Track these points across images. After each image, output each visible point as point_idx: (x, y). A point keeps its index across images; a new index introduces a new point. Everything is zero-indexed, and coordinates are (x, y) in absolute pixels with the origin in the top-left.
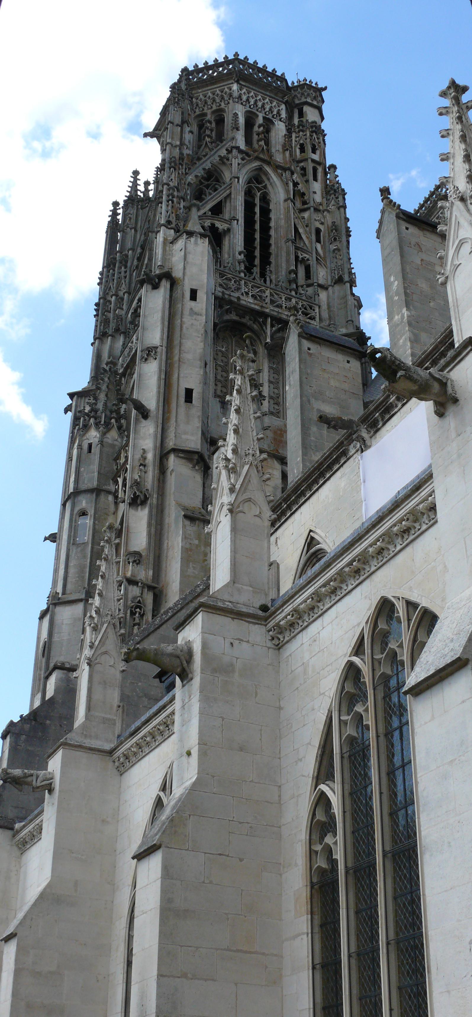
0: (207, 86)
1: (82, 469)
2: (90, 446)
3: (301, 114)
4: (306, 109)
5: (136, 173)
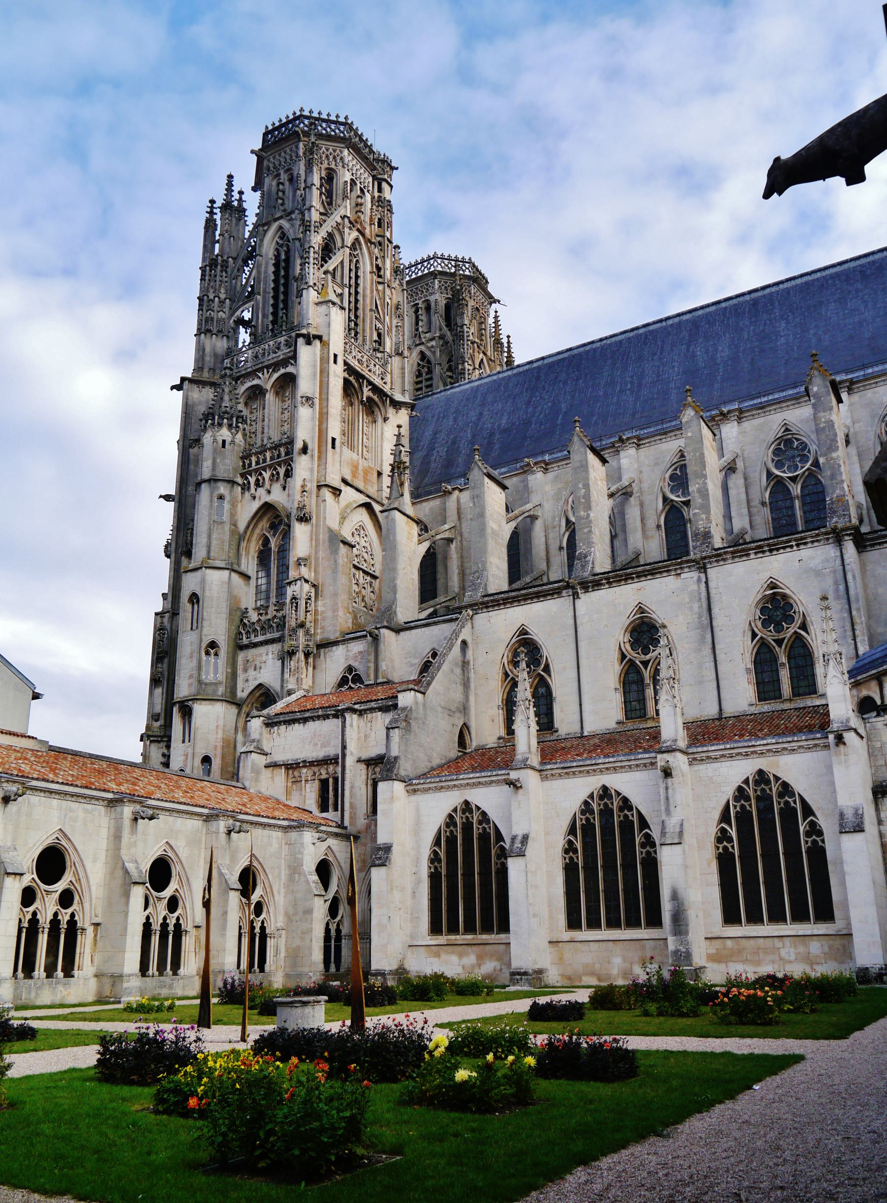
0: (322, 139)
2: (224, 442)
3: (380, 190)
4: (384, 185)
5: (230, 177)
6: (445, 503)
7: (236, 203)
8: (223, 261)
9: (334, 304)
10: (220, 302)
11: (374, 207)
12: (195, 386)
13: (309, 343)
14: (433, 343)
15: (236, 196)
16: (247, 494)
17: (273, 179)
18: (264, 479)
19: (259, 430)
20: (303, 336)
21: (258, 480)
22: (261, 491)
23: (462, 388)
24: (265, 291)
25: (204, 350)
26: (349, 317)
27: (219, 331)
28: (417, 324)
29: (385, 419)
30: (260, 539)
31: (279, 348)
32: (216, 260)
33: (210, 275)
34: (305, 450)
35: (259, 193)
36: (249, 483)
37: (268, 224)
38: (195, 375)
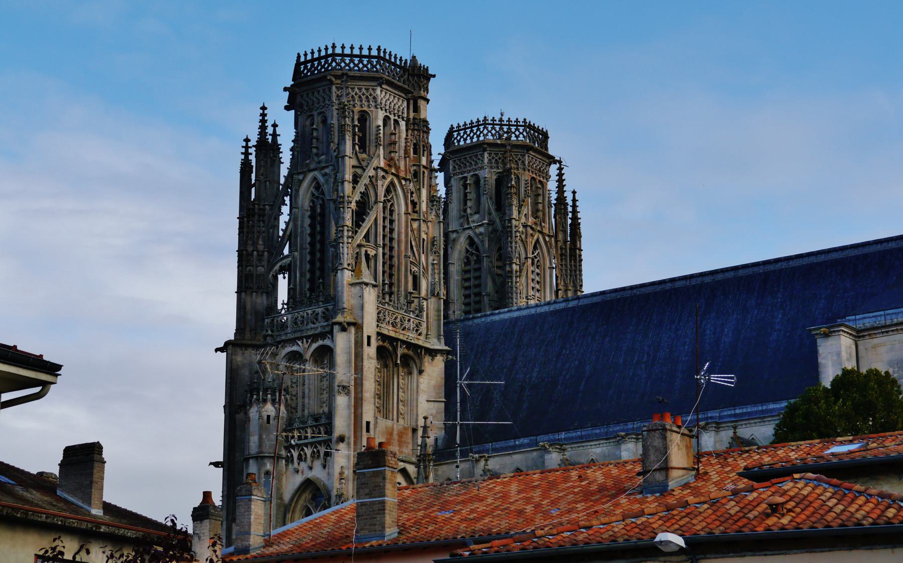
1: (264, 436)
2: (269, 417)
5: (264, 108)
6: (473, 467)
7: (270, 138)
8: (260, 209)
9: (367, 284)
10: (258, 255)
11: (410, 132)
12: (238, 349)
13: (344, 329)
14: (482, 230)
15: (270, 130)
16: (290, 466)
17: (306, 119)
18: (305, 454)
19: (300, 394)
20: (340, 324)
21: (300, 455)
22: (303, 465)
23: (502, 316)
24: (302, 248)
25: (245, 307)
26: (383, 281)
27: (258, 288)
28: (465, 204)
29: (421, 372)
30: (303, 510)
31: (317, 319)
32: (253, 209)
33: (248, 226)
34: (341, 439)
35: (293, 112)
36: (292, 456)
37: (305, 174)
38: (238, 337)
